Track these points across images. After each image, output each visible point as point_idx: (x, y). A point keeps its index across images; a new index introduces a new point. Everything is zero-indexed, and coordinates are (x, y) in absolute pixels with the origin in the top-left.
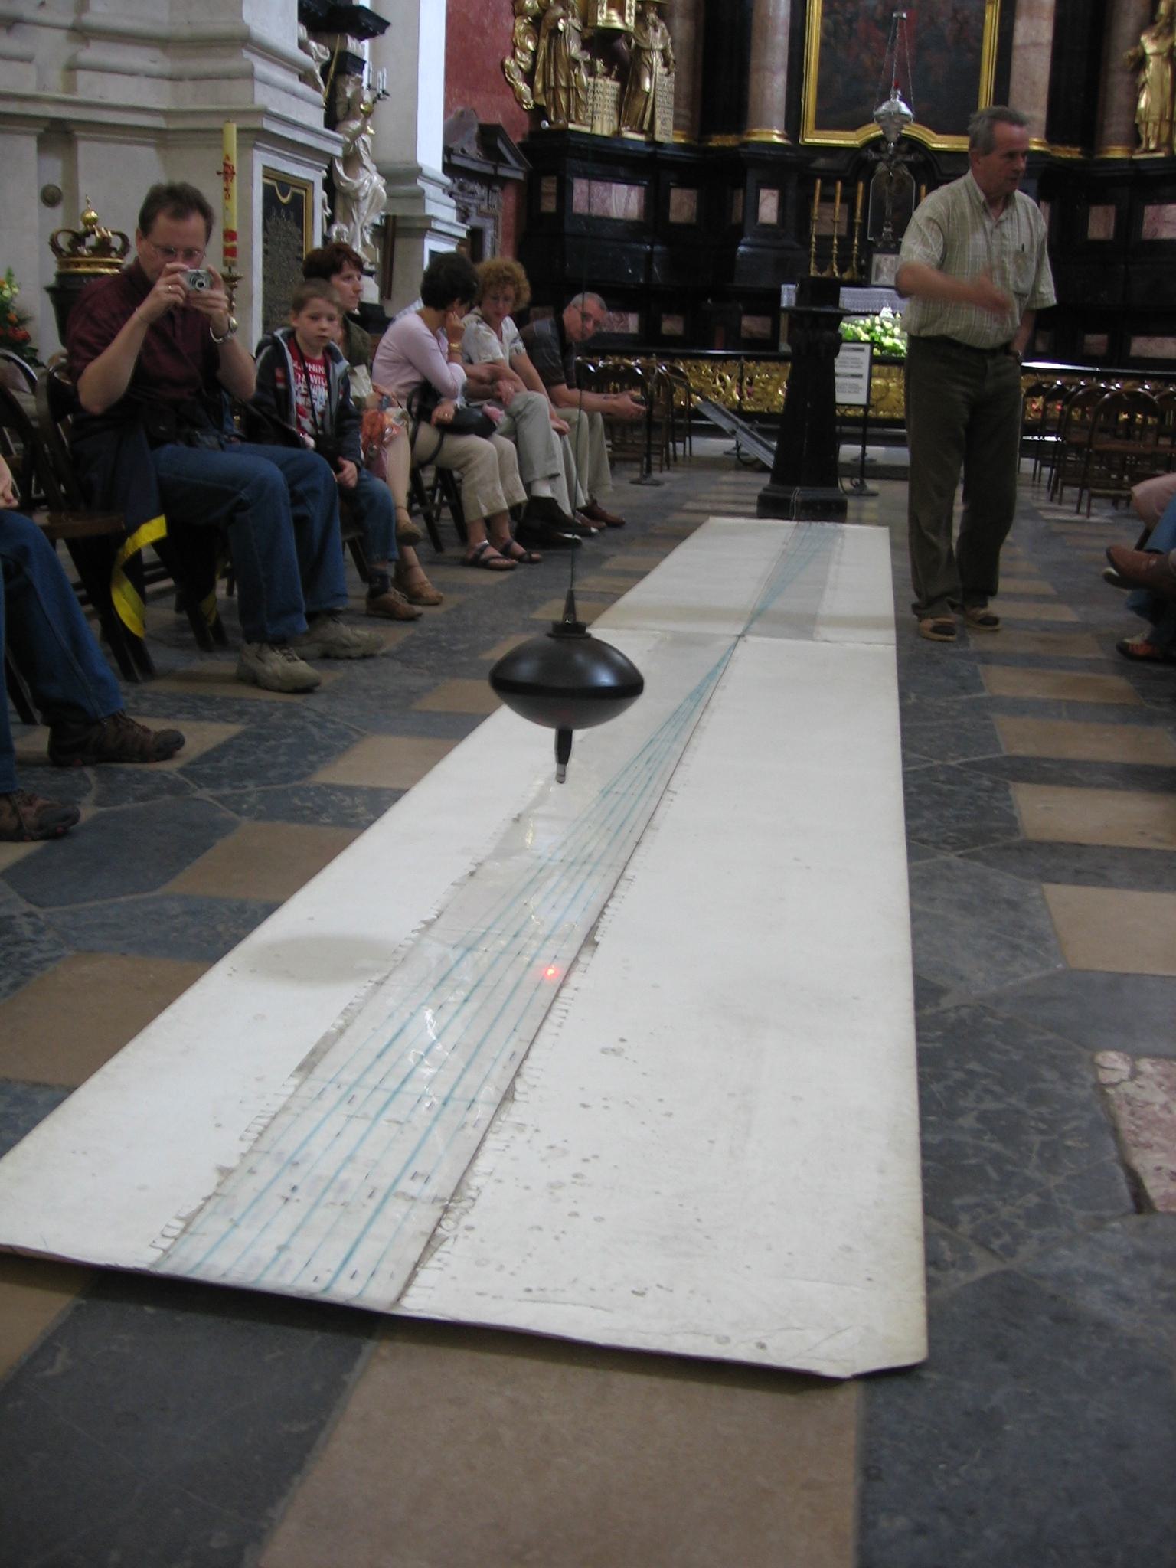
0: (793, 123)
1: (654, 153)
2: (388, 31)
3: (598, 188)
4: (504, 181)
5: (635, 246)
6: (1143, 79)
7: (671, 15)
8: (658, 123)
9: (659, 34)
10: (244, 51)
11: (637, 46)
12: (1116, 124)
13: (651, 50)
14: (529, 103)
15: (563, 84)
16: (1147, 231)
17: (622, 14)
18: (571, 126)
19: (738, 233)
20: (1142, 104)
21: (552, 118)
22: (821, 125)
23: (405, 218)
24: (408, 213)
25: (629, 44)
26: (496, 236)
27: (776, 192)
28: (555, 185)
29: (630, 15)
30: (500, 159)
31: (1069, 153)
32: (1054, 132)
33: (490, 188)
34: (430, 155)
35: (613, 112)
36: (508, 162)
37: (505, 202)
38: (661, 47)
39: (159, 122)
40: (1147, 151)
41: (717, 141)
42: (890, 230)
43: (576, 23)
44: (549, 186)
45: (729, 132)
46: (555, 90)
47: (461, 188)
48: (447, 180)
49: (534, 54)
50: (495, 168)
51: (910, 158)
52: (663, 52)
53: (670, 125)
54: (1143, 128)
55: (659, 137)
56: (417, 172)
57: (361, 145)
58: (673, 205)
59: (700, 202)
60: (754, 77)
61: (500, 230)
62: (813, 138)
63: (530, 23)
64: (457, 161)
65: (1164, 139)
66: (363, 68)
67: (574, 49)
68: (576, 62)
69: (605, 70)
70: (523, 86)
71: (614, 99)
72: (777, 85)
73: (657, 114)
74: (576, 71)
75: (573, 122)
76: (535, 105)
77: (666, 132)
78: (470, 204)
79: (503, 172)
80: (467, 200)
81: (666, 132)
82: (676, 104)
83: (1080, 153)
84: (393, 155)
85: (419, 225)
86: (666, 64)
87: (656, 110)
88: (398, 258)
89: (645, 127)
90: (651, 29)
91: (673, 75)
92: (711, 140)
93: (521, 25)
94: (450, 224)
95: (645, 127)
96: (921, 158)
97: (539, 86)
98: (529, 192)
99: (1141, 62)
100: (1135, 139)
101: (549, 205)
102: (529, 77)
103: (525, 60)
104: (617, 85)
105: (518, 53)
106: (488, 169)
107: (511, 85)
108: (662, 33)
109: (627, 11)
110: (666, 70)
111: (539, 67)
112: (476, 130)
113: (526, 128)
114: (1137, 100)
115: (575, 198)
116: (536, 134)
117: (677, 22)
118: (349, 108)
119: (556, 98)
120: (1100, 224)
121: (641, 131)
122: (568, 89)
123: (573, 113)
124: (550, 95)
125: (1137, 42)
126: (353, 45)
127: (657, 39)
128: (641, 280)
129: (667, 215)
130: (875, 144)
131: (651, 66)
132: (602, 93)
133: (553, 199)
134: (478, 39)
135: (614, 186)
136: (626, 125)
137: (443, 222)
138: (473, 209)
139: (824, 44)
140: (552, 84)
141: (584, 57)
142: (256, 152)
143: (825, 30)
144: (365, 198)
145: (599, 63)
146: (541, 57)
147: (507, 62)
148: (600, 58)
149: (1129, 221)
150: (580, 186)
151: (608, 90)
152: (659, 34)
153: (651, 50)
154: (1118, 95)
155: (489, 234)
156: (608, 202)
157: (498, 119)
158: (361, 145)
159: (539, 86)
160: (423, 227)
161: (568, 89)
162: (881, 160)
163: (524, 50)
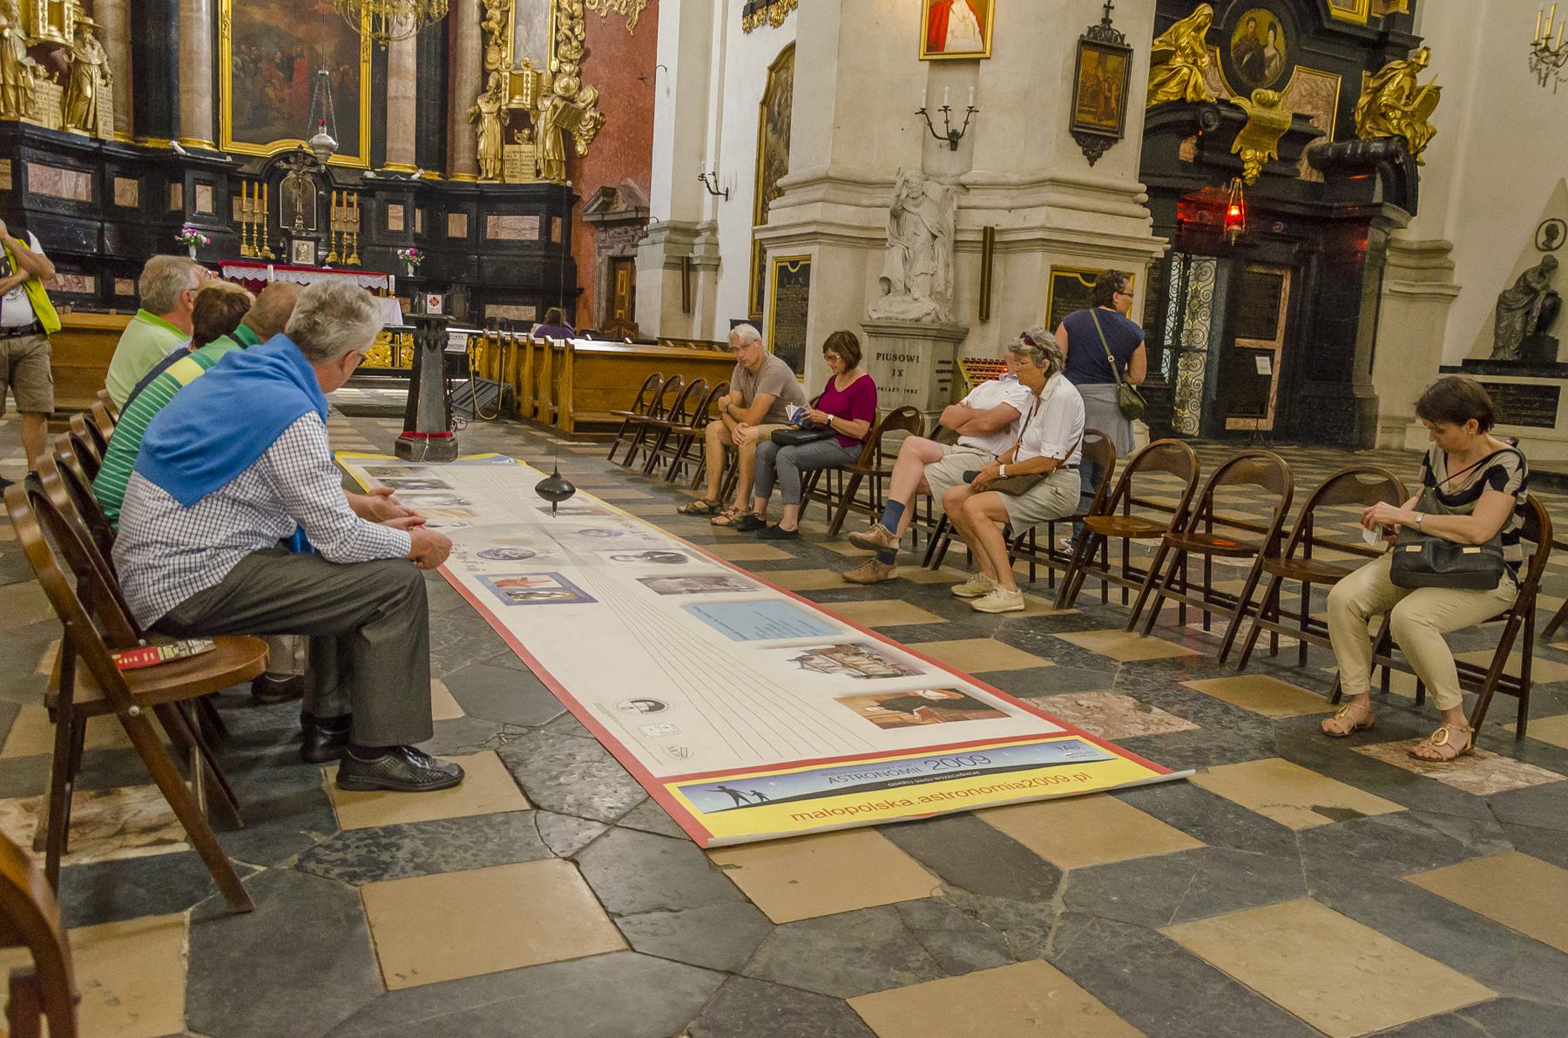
1: (100, 148)
7: (104, 38)
8: (100, 124)
9: (95, 52)
11: (76, 58)
12: (463, 158)
15: (12, 83)
16: (490, 235)
17: (61, 30)
19: (180, 217)
20: (481, 146)
25: (70, 57)
27: (210, 188)
29: (69, 33)
31: (434, 176)
32: (421, 162)
35: (59, 111)
40: (485, 179)
41: (152, 143)
43: (21, 34)
45: (162, 137)
52: (101, 66)
55: (101, 136)
58: (117, 192)
59: (140, 189)
60: (184, 98)
62: (230, 146)
65: (497, 172)
67: (20, 54)
68: (23, 66)
69: (47, 75)
71: (59, 100)
72: (206, 103)
73: (99, 117)
75: (23, 115)
77: (109, 130)
81: (109, 130)
86: (104, 77)
87: (98, 113)
89: (89, 126)
90: (88, 46)
91: (110, 86)
92: (147, 142)
95: (89, 126)
99: (477, 118)
104: (61, 88)
108: (99, 52)
109: (67, 30)
110: (104, 82)
114: (477, 143)
117: (110, 44)
120: (457, 226)
121: (86, 129)
123: (22, 108)
125: (475, 103)
127: (94, 56)
128: (95, 250)
129: (113, 201)
136: (71, 122)
139: (234, 76)
141: (30, 62)
143: (235, 65)
145: (41, 69)
148: (41, 64)
149: (477, 226)
152: (95, 52)
154: (464, 139)
156: (59, 184)
161: (16, 87)
162: (291, 169)
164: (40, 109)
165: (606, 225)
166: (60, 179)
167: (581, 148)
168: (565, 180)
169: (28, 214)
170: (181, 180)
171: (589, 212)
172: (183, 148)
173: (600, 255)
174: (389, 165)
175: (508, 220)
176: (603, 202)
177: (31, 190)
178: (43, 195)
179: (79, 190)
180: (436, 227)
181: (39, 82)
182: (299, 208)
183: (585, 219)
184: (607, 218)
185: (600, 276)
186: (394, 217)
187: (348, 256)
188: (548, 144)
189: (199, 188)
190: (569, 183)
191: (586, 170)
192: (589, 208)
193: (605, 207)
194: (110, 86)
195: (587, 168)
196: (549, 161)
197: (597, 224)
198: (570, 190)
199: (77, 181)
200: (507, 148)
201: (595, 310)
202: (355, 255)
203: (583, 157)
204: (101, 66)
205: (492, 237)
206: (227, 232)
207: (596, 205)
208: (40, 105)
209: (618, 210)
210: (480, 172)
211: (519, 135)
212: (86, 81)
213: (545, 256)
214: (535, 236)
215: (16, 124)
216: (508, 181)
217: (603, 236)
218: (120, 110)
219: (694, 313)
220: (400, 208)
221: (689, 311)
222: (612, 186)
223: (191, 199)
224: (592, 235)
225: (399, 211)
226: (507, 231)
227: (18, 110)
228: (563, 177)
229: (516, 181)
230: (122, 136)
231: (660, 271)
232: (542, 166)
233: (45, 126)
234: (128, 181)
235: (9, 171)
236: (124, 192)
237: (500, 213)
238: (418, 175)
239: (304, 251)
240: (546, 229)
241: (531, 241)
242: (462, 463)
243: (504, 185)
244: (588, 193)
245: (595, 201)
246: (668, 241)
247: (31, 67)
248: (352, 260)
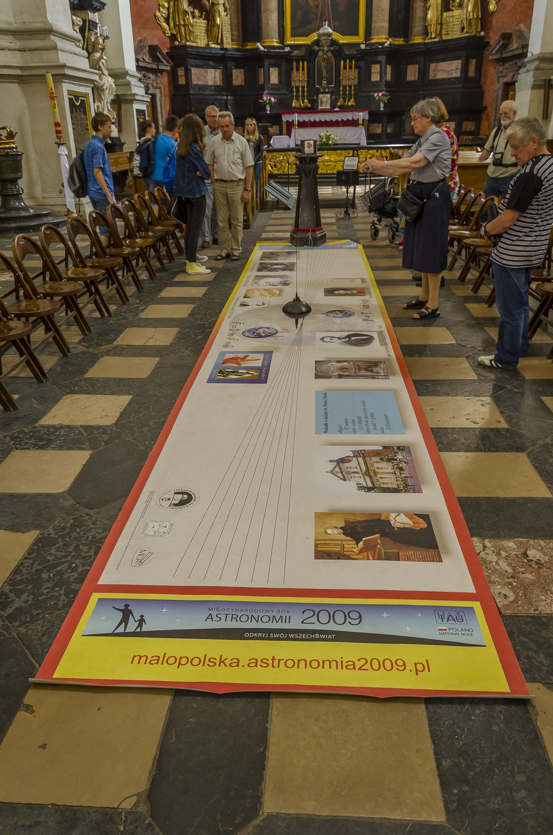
0: (282, 37)
1: (224, 54)
2: (106, 7)
3: (202, 71)
4: (162, 71)
5: (219, 97)
6: (429, 4)
8: (224, 39)
10: (51, 36)
12: (417, 27)
13: (218, 4)
15: (182, 23)
16: (431, 77)
18: (188, 43)
19: (262, 88)
20: (429, 16)
21: (179, 40)
22: (293, 35)
24: (125, 93)
26: (161, 97)
27: (277, 69)
28: (184, 72)
30: (158, 61)
31: (400, 41)
32: (392, 33)
33: (156, 75)
34: (130, 65)
35: (205, 35)
36: (163, 63)
37: (164, 80)
38: (223, 2)
39: (18, 72)
40: (431, 38)
41: (250, 46)
42: (325, 82)
44: (181, 72)
46: (179, 26)
47: (144, 76)
48: (139, 75)
49: (168, 9)
50: (158, 65)
51: (332, 49)
52: (224, 4)
53: (229, 40)
54: (429, 27)
55: (226, 46)
56: (126, 73)
57: (101, 64)
60: (264, 15)
64: (141, 64)
65: (438, 32)
66: (97, 27)
68: (187, 12)
69: (200, 15)
70: (164, 25)
71: (205, 29)
72: (274, 17)
73: (224, 35)
74: (187, 17)
75: (188, 41)
76: (171, 33)
77: (228, 44)
78: (149, 83)
79: (161, 67)
80: (147, 81)
81: (228, 44)
82: (232, 30)
83: (403, 41)
84: (115, 65)
85: (130, 98)
86: (225, 11)
87: (223, 33)
88: (123, 112)
89: (219, 41)
91: (229, 15)
92: (247, 46)
94: (143, 96)
95: (219, 41)
96: (337, 48)
98: (173, 75)
100: (426, 33)
101: (182, 81)
102: (167, 20)
104: (206, 22)
105: (161, 9)
106: (155, 66)
107: (160, 25)
110: (226, 13)
111: (171, 15)
112: (147, 48)
113: (168, 45)
115: (193, 77)
116: (173, 48)
118: (94, 47)
121: (218, 44)
122: (184, 25)
123: (188, 37)
124: (177, 28)
130: (317, 42)
131: (219, 12)
132: (199, 26)
133: (184, 78)
134: (143, 3)
135: (208, 70)
136: (210, 41)
137: (140, 95)
138: (150, 85)
140: (178, 23)
141: (189, 9)
142: (63, 84)
144: (106, 89)
145: (197, 12)
146: (171, 11)
147: (157, 14)
148: (197, 9)
149: (424, 72)
150: (194, 71)
151: (202, 25)
153: (218, 4)
154: (418, 13)
155: (158, 96)
156: (207, 77)
157: (156, 42)
158: (101, 64)
159: (172, 25)
160: (131, 100)
161: (184, 25)
162: (320, 50)
163: (164, 7)
164: (196, 35)
165: (503, 61)
166: (207, 75)
167: (492, 7)
168: (480, 32)
169: (192, 97)
170: (262, 66)
171: (494, 52)
172: (263, 46)
173: (498, 82)
174: (373, 39)
175: (443, 65)
176: (503, 44)
177: (194, 83)
178: (200, 85)
179: (216, 79)
180: (400, 74)
181: (195, 20)
182: (324, 74)
183: (491, 58)
184: (504, 55)
185: (497, 97)
186: (374, 73)
187: (349, 101)
188: (470, 8)
189: (272, 70)
190: (482, 33)
191: (494, 22)
192: (493, 49)
193: (504, 47)
194: (229, 15)
195: (495, 22)
196: (470, 20)
197: (497, 61)
198: (483, 38)
199: (215, 74)
200: (445, 14)
201: (493, 121)
202: (352, 100)
203: (493, 13)
204: (224, 4)
205: (433, 78)
206: (285, 94)
207: (498, 47)
208: (196, 34)
209: (512, 48)
210: (427, 34)
211: (453, 4)
212: (217, 15)
213: (463, 87)
214: (458, 74)
215: (185, 46)
216: (445, 38)
217: (501, 69)
218: (234, 29)
219: (550, 120)
220: (378, 66)
221: (547, 118)
222: (510, 32)
223: (267, 76)
224: (495, 68)
225: (377, 68)
226: (441, 73)
227: (186, 38)
228: (479, 30)
229: (449, 37)
230: (236, 45)
231: (529, 91)
232: (465, 24)
233: (199, 45)
234: (239, 70)
235: (184, 74)
236: (237, 76)
237: (438, 61)
238: (388, 43)
239: (325, 100)
240: (465, 69)
241: (456, 78)
242: (326, 248)
243: (442, 41)
244: (494, 39)
245: (497, 44)
246: (537, 69)
247: (191, 12)
248: (351, 103)
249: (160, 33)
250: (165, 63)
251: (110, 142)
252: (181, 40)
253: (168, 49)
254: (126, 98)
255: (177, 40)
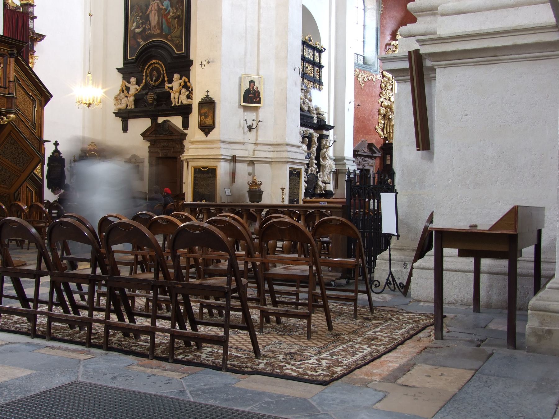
4: (375, 157)
14: (383, 136)
15: (391, 131)
23: (340, 169)
26: (373, 171)
39: (270, 160)
46: (389, 132)
47: (363, 159)
49: (384, 124)
50: (372, 154)
56: (344, 159)
57: (326, 155)
61: (375, 169)
63: (383, 117)
70: (382, 133)
78: (365, 163)
79: (374, 155)
84: (339, 155)
93: (380, 117)
97: (385, 132)
102: (383, 130)
103: (382, 125)
105: (379, 124)
106: (370, 154)
107: (378, 132)
111: (385, 127)
112: (367, 145)
113: (382, 143)
116: (385, 144)
119: (390, 135)
126: (325, 132)
133: (389, 161)
146: (385, 125)
147: (376, 127)
157: (374, 142)
159: (385, 132)
163: (381, 123)
249: (378, 137)
250: (378, 152)
251: (324, 192)
252: (390, 140)
253: (382, 145)
254: (342, 171)
255: (387, 140)
